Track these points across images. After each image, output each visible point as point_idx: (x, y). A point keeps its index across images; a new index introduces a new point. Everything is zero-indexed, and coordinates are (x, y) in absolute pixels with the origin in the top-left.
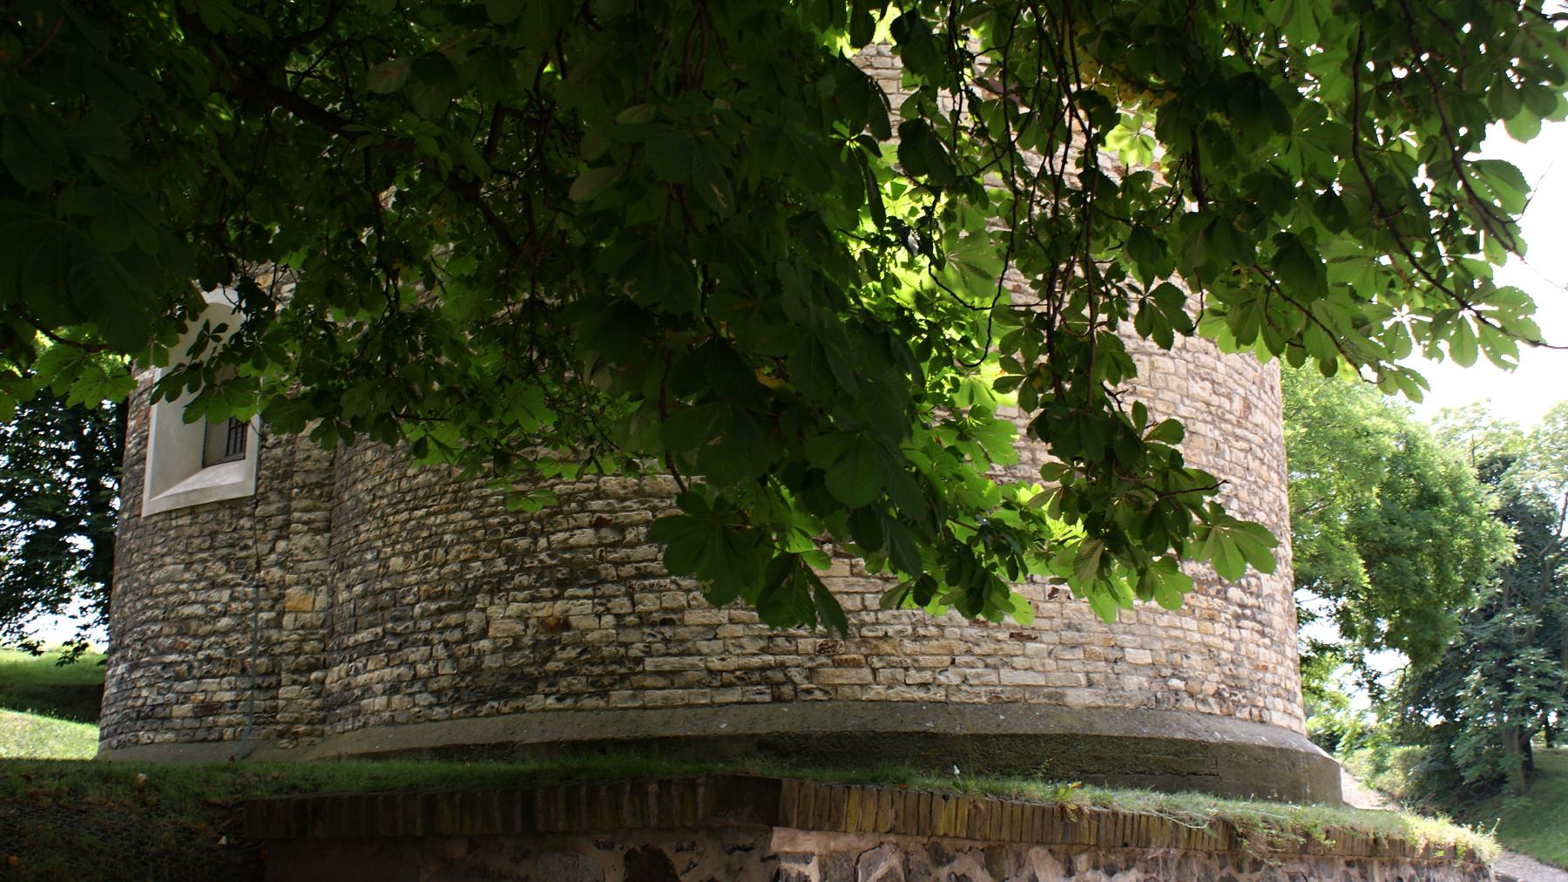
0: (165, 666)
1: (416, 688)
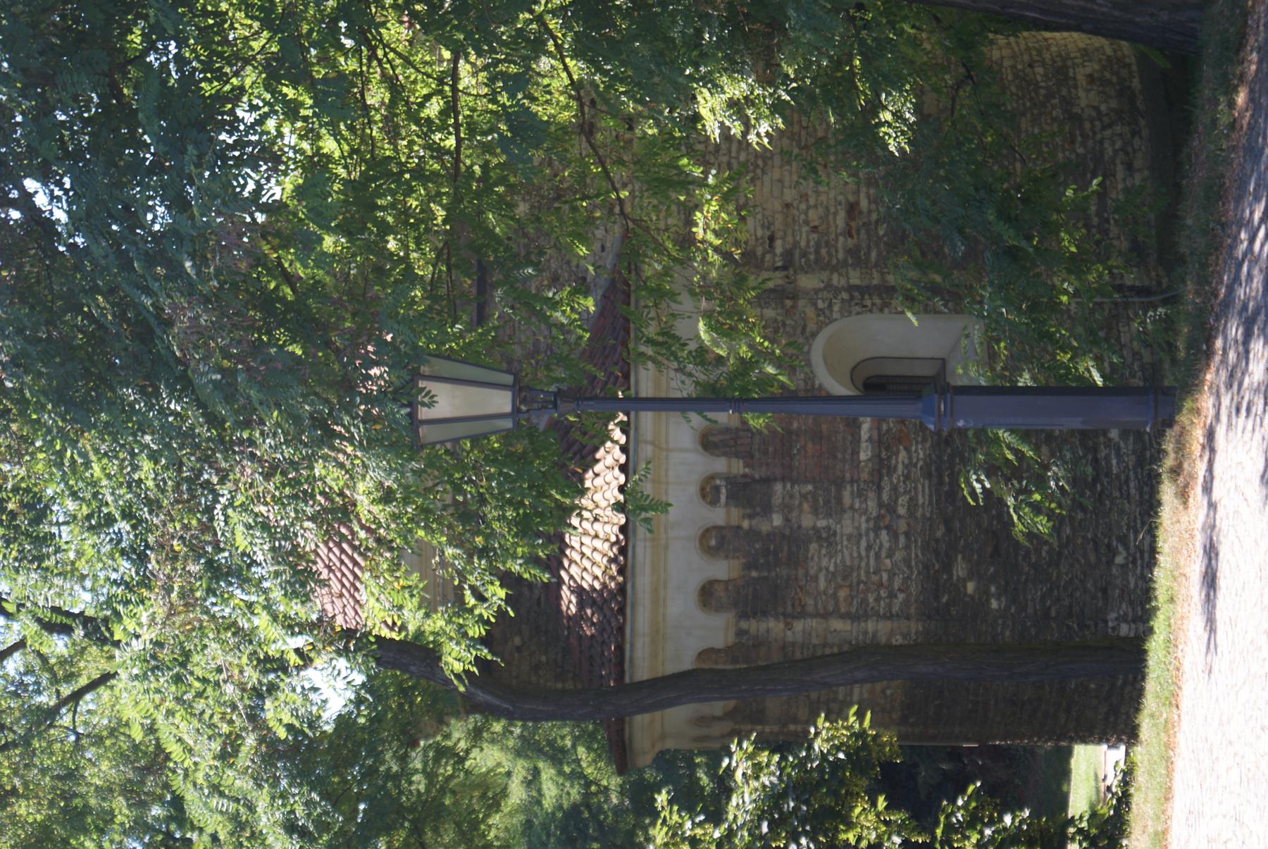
1: (1130, 150)
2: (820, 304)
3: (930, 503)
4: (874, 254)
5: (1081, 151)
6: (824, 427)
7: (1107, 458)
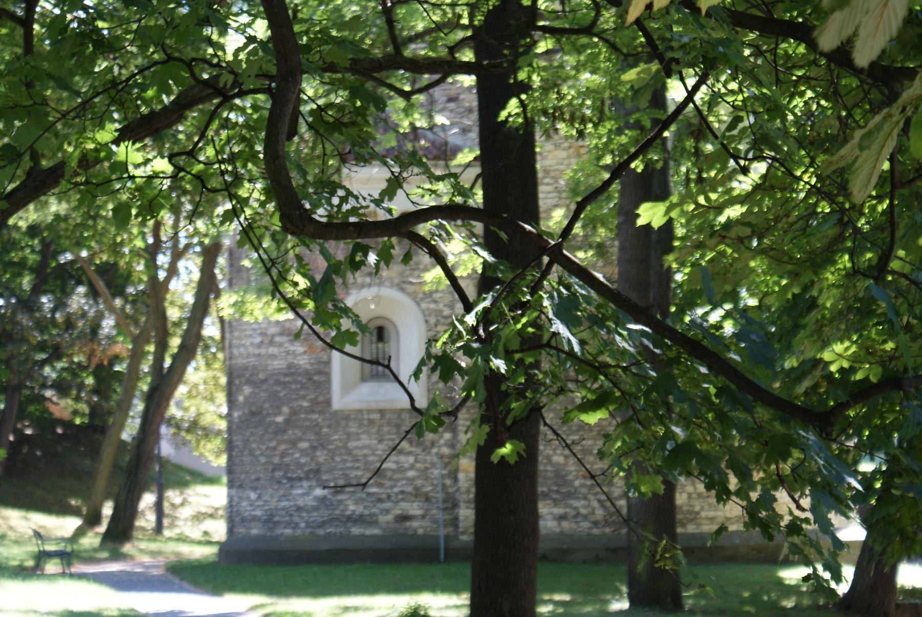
5: (577, 483)
7: (302, 486)
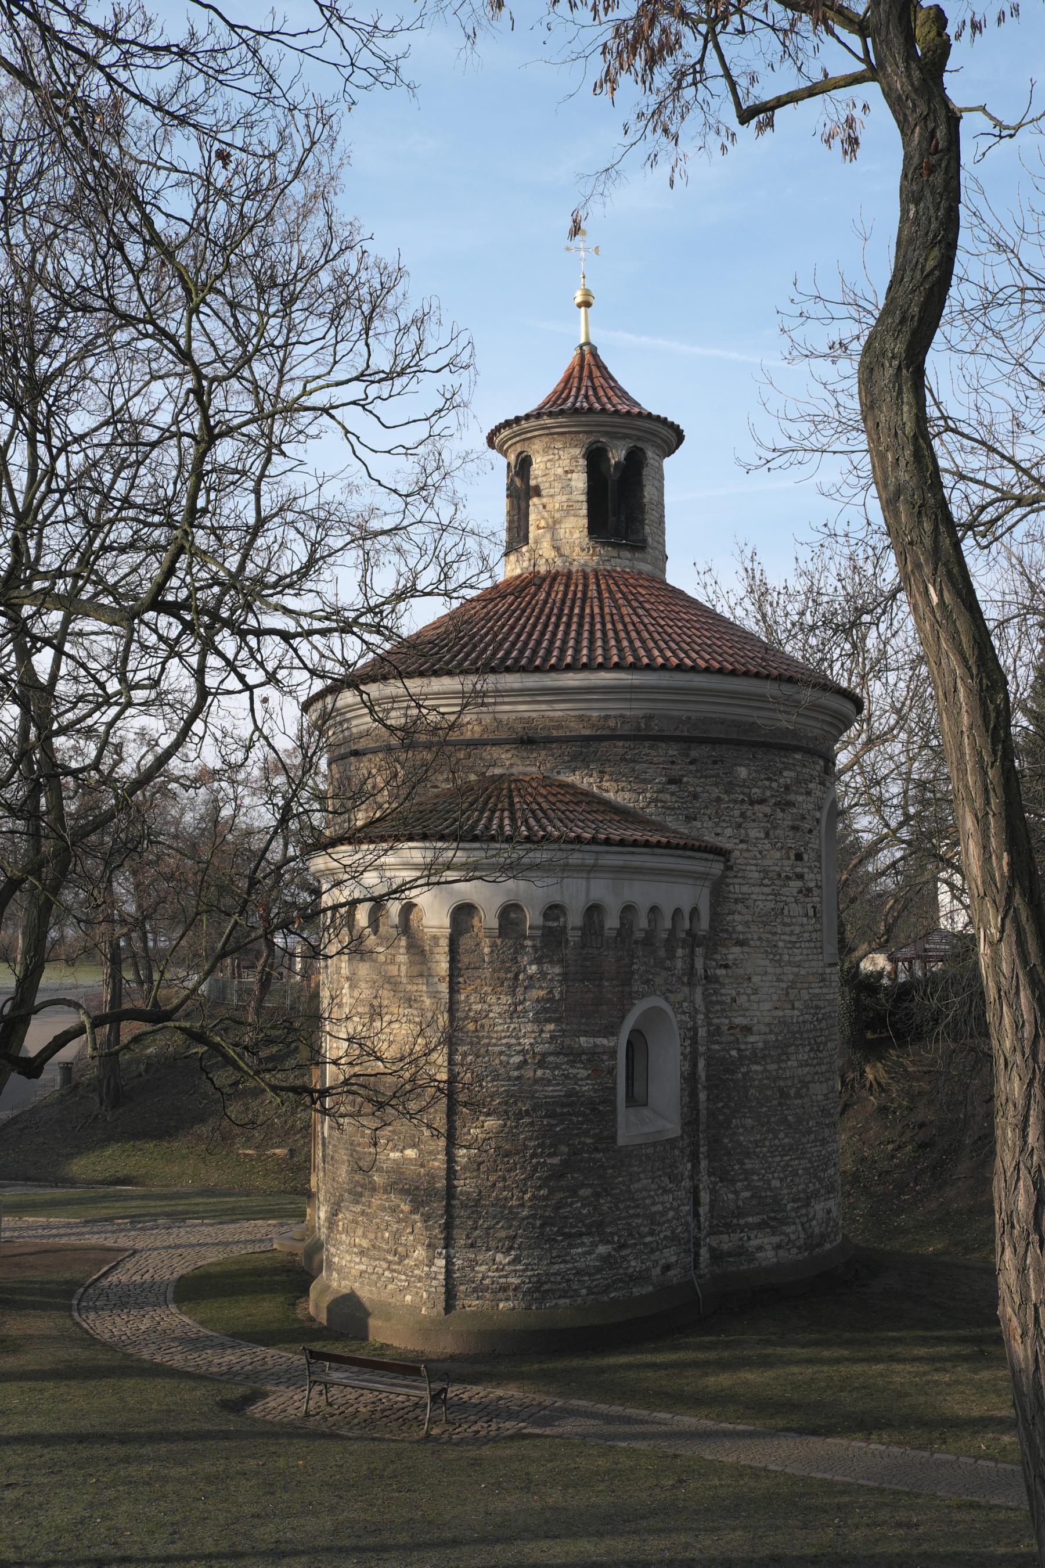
0: (645, 1245)
2: (685, 1004)
3: (546, 1097)
4: (716, 1047)
5: (789, 1207)
6: (605, 1007)
7: (583, 1244)
